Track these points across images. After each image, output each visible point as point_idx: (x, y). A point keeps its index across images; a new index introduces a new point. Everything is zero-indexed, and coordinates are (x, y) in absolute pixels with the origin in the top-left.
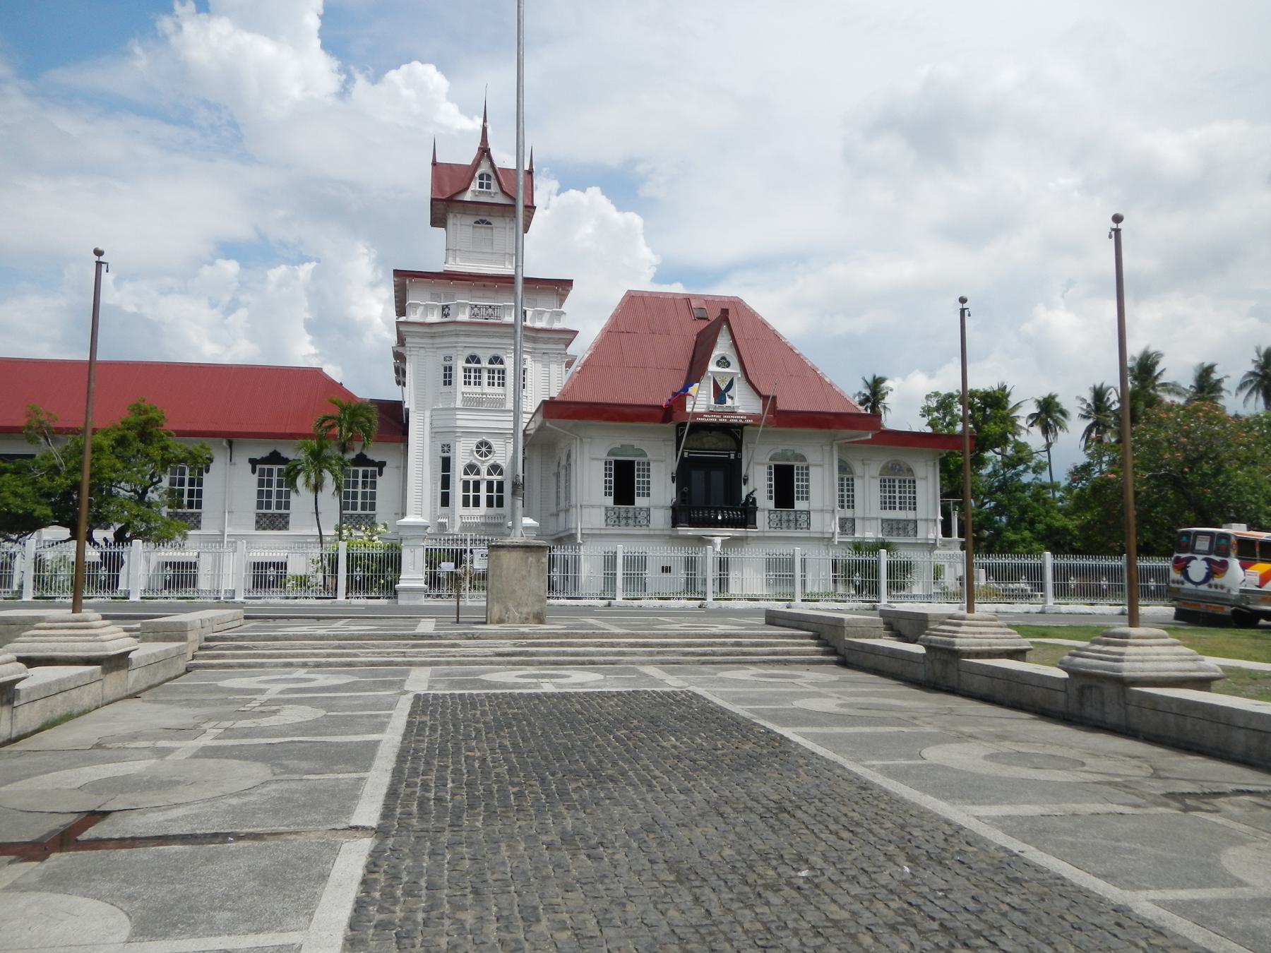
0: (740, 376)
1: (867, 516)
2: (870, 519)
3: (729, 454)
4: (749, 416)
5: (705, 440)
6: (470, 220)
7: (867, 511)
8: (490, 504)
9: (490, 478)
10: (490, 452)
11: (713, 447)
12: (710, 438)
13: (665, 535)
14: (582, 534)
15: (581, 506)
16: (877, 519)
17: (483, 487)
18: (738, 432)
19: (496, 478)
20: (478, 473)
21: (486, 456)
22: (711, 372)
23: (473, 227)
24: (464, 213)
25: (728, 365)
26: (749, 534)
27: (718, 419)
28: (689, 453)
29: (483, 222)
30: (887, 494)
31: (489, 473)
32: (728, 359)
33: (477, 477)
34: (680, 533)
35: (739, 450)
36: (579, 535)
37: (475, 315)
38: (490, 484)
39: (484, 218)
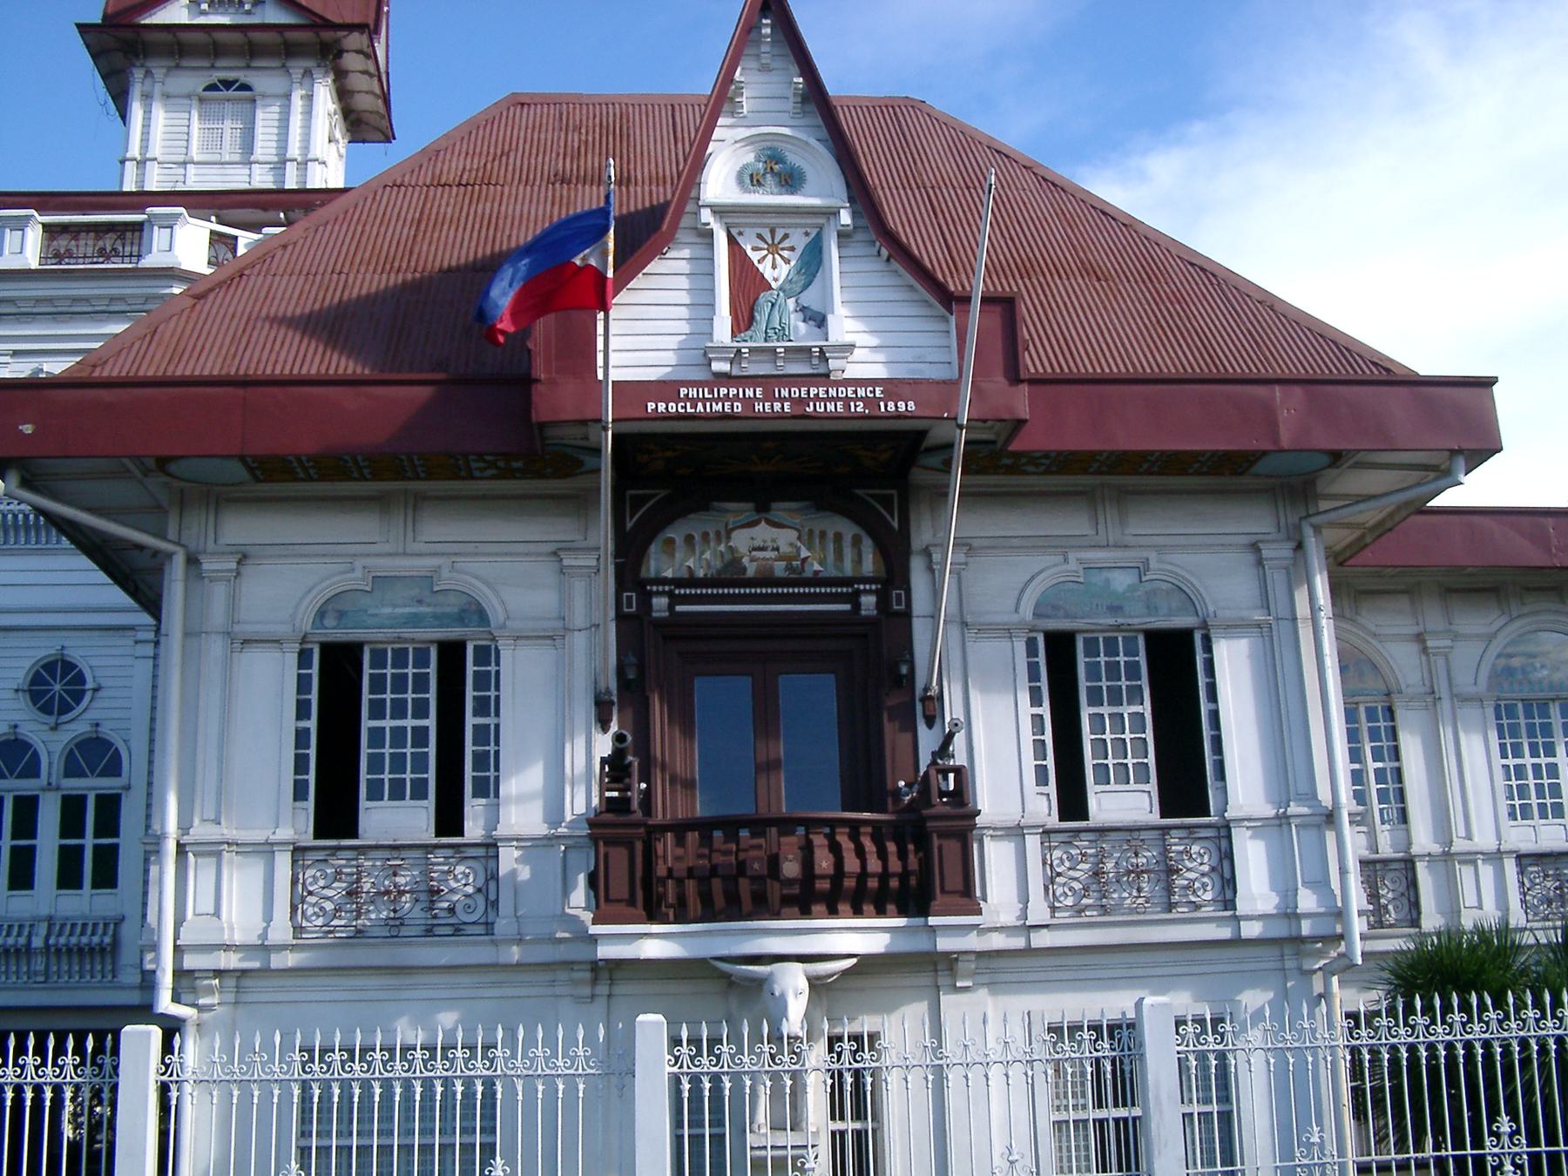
0: (846, 218)
1: (1459, 845)
2: (1470, 858)
3: (854, 598)
4: (893, 387)
5: (742, 540)
6: (193, 81)
7: (1458, 828)
8: (69, 877)
9: (75, 785)
10: (78, 696)
11: (780, 569)
12: (763, 533)
13: (568, 965)
14: (179, 973)
15: (181, 849)
16: (1496, 857)
17: (49, 817)
18: (887, 502)
19: (91, 786)
20: (33, 770)
21: (65, 708)
22: (720, 211)
23: (201, 100)
24: (178, 67)
25: (790, 180)
26: (944, 944)
27: (748, 402)
28: (675, 600)
29: (228, 84)
30: (1528, 761)
31: (72, 770)
32: (794, 158)
33: (27, 786)
34: (605, 951)
35: (894, 577)
36: (166, 980)
37: (59, 258)
38: (72, 810)
39: (230, 75)
